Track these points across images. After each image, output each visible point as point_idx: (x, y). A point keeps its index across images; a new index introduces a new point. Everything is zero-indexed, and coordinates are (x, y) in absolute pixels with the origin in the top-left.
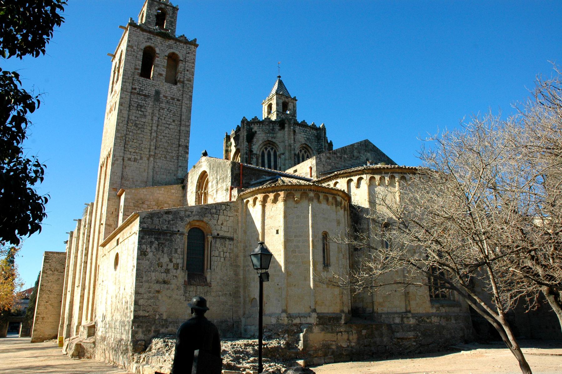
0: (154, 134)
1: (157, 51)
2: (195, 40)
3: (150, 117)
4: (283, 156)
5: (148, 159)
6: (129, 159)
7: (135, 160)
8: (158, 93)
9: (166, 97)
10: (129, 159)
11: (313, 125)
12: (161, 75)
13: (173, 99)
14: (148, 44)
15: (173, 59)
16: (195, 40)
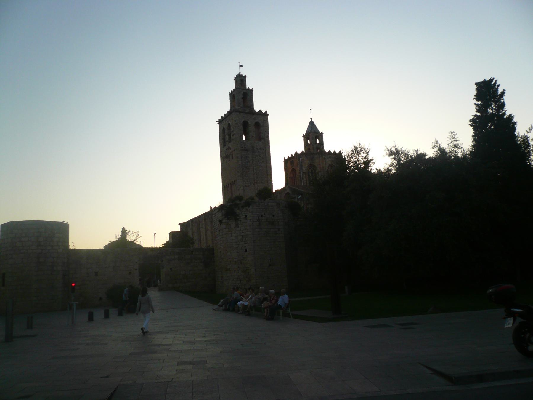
0: (255, 171)
1: (249, 123)
2: (266, 112)
3: (251, 162)
4: (320, 173)
5: (254, 184)
6: (246, 186)
7: (248, 186)
8: (253, 147)
9: (257, 149)
10: (246, 186)
11: (335, 152)
12: (253, 136)
13: (260, 149)
14: (244, 120)
15: (257, 125)
16: (266, 112)
